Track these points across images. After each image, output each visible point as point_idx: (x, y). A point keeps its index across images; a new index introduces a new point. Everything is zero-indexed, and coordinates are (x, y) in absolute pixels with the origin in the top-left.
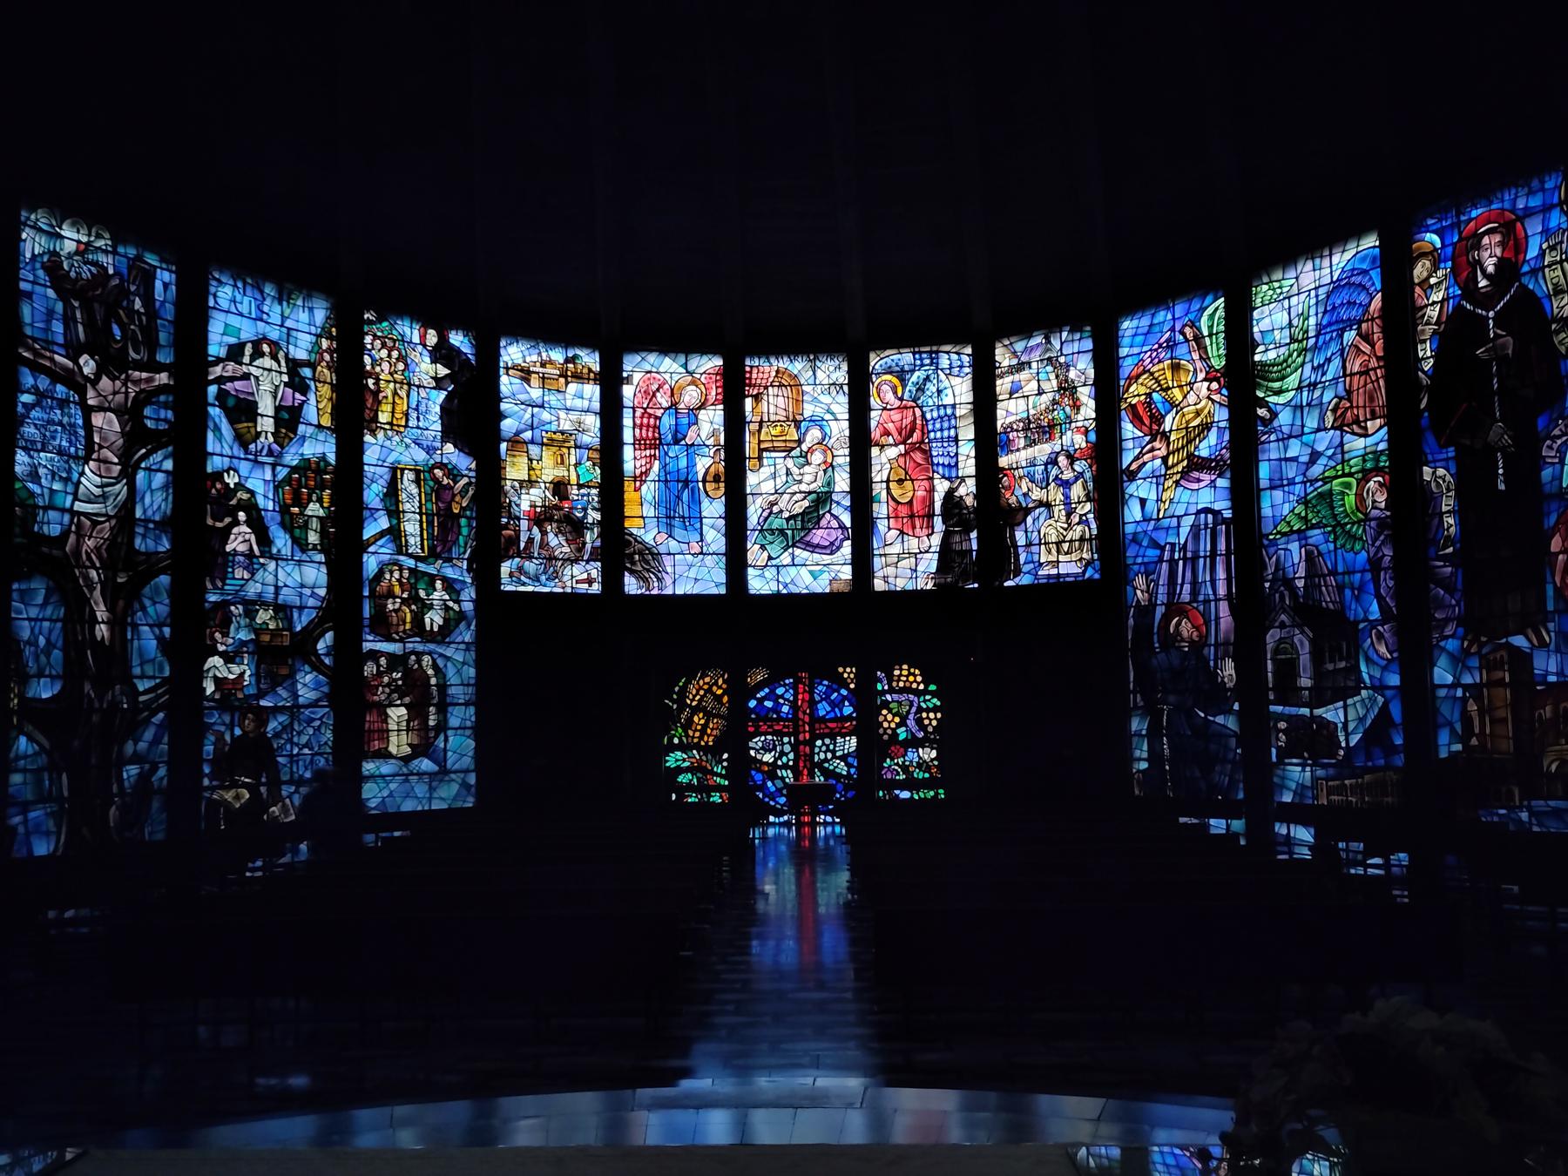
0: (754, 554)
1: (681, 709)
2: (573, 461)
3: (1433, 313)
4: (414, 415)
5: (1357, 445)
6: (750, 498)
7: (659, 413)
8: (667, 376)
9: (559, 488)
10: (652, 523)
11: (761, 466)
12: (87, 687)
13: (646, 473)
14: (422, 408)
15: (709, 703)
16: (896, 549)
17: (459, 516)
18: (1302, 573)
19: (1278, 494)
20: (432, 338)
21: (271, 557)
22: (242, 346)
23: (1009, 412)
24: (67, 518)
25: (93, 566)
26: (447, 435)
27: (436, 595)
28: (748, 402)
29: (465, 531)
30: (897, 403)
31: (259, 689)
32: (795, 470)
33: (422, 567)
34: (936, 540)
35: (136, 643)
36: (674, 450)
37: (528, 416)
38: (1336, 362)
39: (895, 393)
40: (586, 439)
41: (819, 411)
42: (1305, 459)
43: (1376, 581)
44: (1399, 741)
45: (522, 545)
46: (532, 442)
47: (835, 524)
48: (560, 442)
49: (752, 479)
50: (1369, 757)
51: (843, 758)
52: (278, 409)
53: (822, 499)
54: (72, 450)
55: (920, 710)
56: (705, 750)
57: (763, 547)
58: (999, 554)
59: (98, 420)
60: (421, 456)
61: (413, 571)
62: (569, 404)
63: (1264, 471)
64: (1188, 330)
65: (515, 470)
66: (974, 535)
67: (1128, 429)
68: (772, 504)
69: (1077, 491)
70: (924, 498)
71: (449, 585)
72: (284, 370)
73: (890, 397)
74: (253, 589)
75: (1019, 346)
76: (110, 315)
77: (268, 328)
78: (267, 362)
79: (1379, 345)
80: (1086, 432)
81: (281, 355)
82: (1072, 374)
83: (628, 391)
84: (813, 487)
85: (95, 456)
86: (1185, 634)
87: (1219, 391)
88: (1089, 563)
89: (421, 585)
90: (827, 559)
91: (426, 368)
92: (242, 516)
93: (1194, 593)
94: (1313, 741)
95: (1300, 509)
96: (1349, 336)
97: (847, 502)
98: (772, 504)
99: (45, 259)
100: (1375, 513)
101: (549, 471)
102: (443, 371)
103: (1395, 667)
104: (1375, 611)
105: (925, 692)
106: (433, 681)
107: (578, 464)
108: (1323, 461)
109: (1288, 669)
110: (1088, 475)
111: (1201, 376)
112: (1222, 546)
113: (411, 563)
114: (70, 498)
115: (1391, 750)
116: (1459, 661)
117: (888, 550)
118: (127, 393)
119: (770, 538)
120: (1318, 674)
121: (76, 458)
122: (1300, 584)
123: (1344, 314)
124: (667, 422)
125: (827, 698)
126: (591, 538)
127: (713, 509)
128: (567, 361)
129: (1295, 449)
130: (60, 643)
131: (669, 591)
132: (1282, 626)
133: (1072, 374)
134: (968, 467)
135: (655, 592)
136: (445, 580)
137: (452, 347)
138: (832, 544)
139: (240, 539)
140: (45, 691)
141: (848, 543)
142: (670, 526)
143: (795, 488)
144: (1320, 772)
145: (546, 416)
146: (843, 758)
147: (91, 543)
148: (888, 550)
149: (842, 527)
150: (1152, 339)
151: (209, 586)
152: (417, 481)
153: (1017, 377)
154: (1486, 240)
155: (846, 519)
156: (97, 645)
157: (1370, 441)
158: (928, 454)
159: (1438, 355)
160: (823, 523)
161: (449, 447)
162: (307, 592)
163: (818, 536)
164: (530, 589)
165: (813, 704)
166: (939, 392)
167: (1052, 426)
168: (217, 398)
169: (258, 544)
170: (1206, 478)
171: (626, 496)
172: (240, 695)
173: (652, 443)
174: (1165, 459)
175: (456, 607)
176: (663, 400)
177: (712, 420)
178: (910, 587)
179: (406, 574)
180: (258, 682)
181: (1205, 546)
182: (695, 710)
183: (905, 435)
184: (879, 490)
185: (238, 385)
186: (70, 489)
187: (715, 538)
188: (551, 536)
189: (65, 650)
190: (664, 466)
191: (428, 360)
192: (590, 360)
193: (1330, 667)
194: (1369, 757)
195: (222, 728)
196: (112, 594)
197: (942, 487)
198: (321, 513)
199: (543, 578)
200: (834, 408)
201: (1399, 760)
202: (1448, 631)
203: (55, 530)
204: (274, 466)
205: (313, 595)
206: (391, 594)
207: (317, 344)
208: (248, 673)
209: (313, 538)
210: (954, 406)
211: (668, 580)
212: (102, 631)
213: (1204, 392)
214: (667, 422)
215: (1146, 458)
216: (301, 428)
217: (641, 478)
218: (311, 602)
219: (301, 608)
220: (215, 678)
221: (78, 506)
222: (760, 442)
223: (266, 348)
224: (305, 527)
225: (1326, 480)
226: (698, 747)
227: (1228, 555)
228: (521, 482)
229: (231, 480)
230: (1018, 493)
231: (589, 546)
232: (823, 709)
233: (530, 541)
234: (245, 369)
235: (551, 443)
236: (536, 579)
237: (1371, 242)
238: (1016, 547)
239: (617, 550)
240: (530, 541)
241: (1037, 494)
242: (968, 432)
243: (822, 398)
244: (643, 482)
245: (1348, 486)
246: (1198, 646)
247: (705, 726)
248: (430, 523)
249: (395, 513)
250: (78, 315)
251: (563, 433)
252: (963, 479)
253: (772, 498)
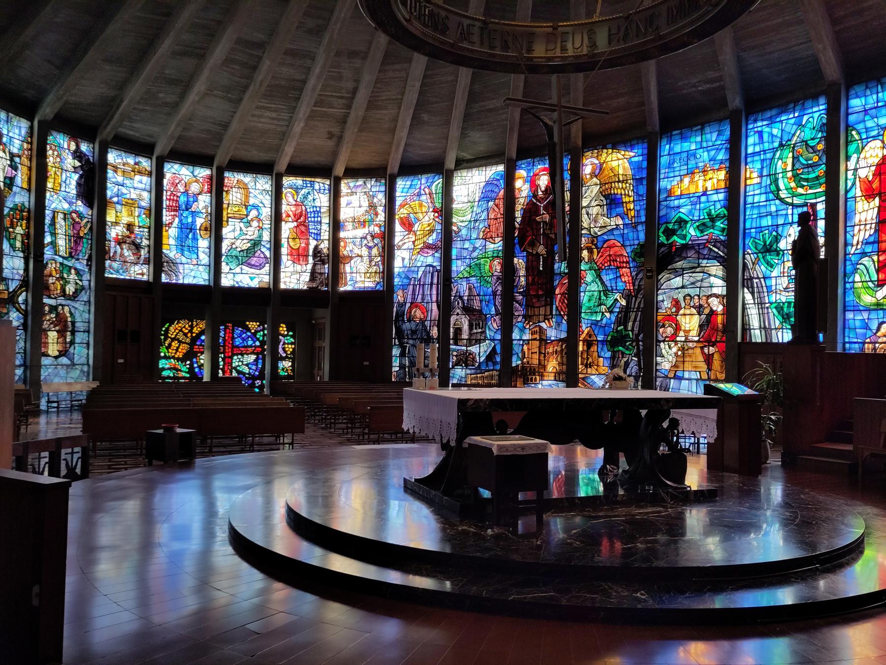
0: (225, 268)
1: (165, 339)
2: (137, 214)
3: (522, 201)
4: (64, 185)
5: (491, 246)
7: (179, 194)
8: (183, 177)
9: (130, 227)
10: (174, 248)
13: (171, 223)
14: (68, 182)
15: (181, 336)
17: (82, 238)
18: (467, 294)
19: (459, 262)
20: (73, 146)
23: (345, 213)
26: (79, 195)
27: (72, 277)
29: (85, 245)
30: (294, 203)
32: (244, 229)
33: (66, 262)
34: (309, 267)
36: (185, 214)
37: (116, 190)
38: (485, 213)
40: (143, 204)
41: (257, 202)
42: (471, 249)
43: (494, 299)
44: (498, 359)
45: (112, 254)
46: (118, 203)
47: (262, 256)
48: (131, 204)
49: (225, 231)
50: (487, 365)
51: (247, 365)
53: (256, 243)
55: (284, 343)
56: (178, 359)
57: (227, 264)
58: (336, 276)
60: (66, 206)
61: (61, 264)
62: (136, 185)
63: (454, 252)
64: (427, 190)
65: (110, 217)
66: (326, 266)
67: (398, 227)
68: (233, 244)
69: (375, 251)
71: (78, 272)
73: (291, 199)
75: (352, 185)
79: (502, 209)
80: (380, 227)
81: (7, 150)
82: (375, 200)
83: (165, 182)
84: (252, 237)
86: (418, 316)
87: (437, 217)
88: (378, 283)
89: (65, 271)
90: (258, 272)
91: (70, 162)
93: (423, 299)
94: (466, 360)
95: (468, 269)
96: (491, 204)
98: (233, 244)
100: (496, 274)
101: (125, 219)
102: (78, 164)
103: (499, 332)
104: (493, 311)
105: (287, 335)
106: (69, 319)
107: (139, 216)
108: (478, 251)
109: (458, 331)
110: (380, 245)
111: (431, 210)
112: (638, 319)
113: (61, 260)
115: (495, 363)
116: (522, 330)
117: (286, 270)
120: (471, 334)
122: (466, 298)
123: (489, 194)
124: (183, 199)
125: (240, 336)
126: (144, 253)
127: (204, 244)
128: (136, 164)
129: (467, 245)
131: (181, 282)
132: (458, 314)
133: (375, 200)
134: (325, 235)
135: (174, 281)
136: (76, 269)
137: (81, 152)
141: (267, 265)
142: (182, 250)
143: (244, 237)
144: (469, 372)
145: (124, 190)
146: (247, 365)
149: (266, 257)
150: (411, 191)
152: (65, 219)
153: (350, 198)
154: (542, 177)
155: (268, 254)
157: (496, 245)
158: (307, 227)
159: (523, 217)
160: (257, 255)
161: (79, 203)
162: (15, 271)
163: (253, 261)
164: (114, 276)
165: (233, 338)
166: (314, 200)
167: (364, 222)
170: (431, 252)
174: (414, 242)
175: (80, 283)
176: (181, 188)
177: (204, 201)
178: (296, 287)
179: (58, 265)
181: (428, 280)
182: (173, 340)
183: (297, 217)
184: (284, 242)
187: (204, 259)
188: (125, 251)
190: (181, 221)
191: (70, 157)
192: (145, 163)
193: (475, 331)
194: (487, 365)
197: (313, 243)
198: (22, 232)
199: (121, 271)
200: (264, 201)
201: (498, 367)
202: (519, 320)
205: (18, 273)
206: (51, 275)
207: (22, 146)
209: (18, 244)
210: (320, 207)
211: (181, 277)
213: (432, 217)
214: (183, 199)
215: (406, 241)
216: (14, 188)
218: (17, 277)
219: (12, 280)
224: (15, 239)
225: (478, 259)
226: (173, 357)
227: (438, 284)
228: (112, 222)
230: (348, 249)
231: (142, 257)
232: (238, 342)
233: (115, 252)
235: (127, 204)
236: (118, 271)
237: (501, 168)
238: (346, 273)
239: (158, 260)
240: (115, 252)
241: (357, 251)
242: (326, 220)
244: (170, 227)
245: (487, 262)
246: (423, 321)
247: (178, 348)
248: (70, 240)
249: (54, 234)
251: (132, 199)
252: (323, 241)
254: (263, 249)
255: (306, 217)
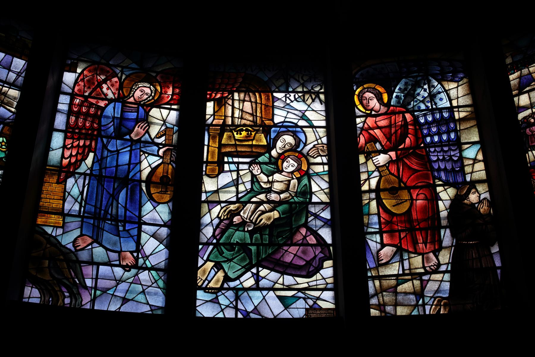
0: (206, 270)
6: (205, 208)
7: (102, 104)
10: (74, 223)
11: (222, 171)
13: (78, 164)
16: (394, 269)
28: (210, 107)
30: (383, 109)
32: (263, 178)
34: (445, 257)
39: (380, 99)
41: (292, 118)
47: (312, 240)
53: (297, 208)
57: (218, 266)
68: (233, 214)
70: (424, 209)
73: (374, 103)
90: (303, 282)
97: (326, 215)
98: (236, 213)
117: (384, 271)
119: (227, 253)
127: (157, 212)
138: (309, 263)
141: (328, 263)
143: (262, 197)
148: (384, 271)
155: (326, 234)
160: (298, 238)
163: (290, 254)
171: (46, 187)
173: (87, 130)
183: (393, 140)
187: (155, 250)
197: (446, 195)
200: (310, 115)
217: (66, 171)
222: (221, 146)
243: (295, 104)
252: (473, 184)
253: (232, 207)
254: (314, 223)
255: (419, 137)
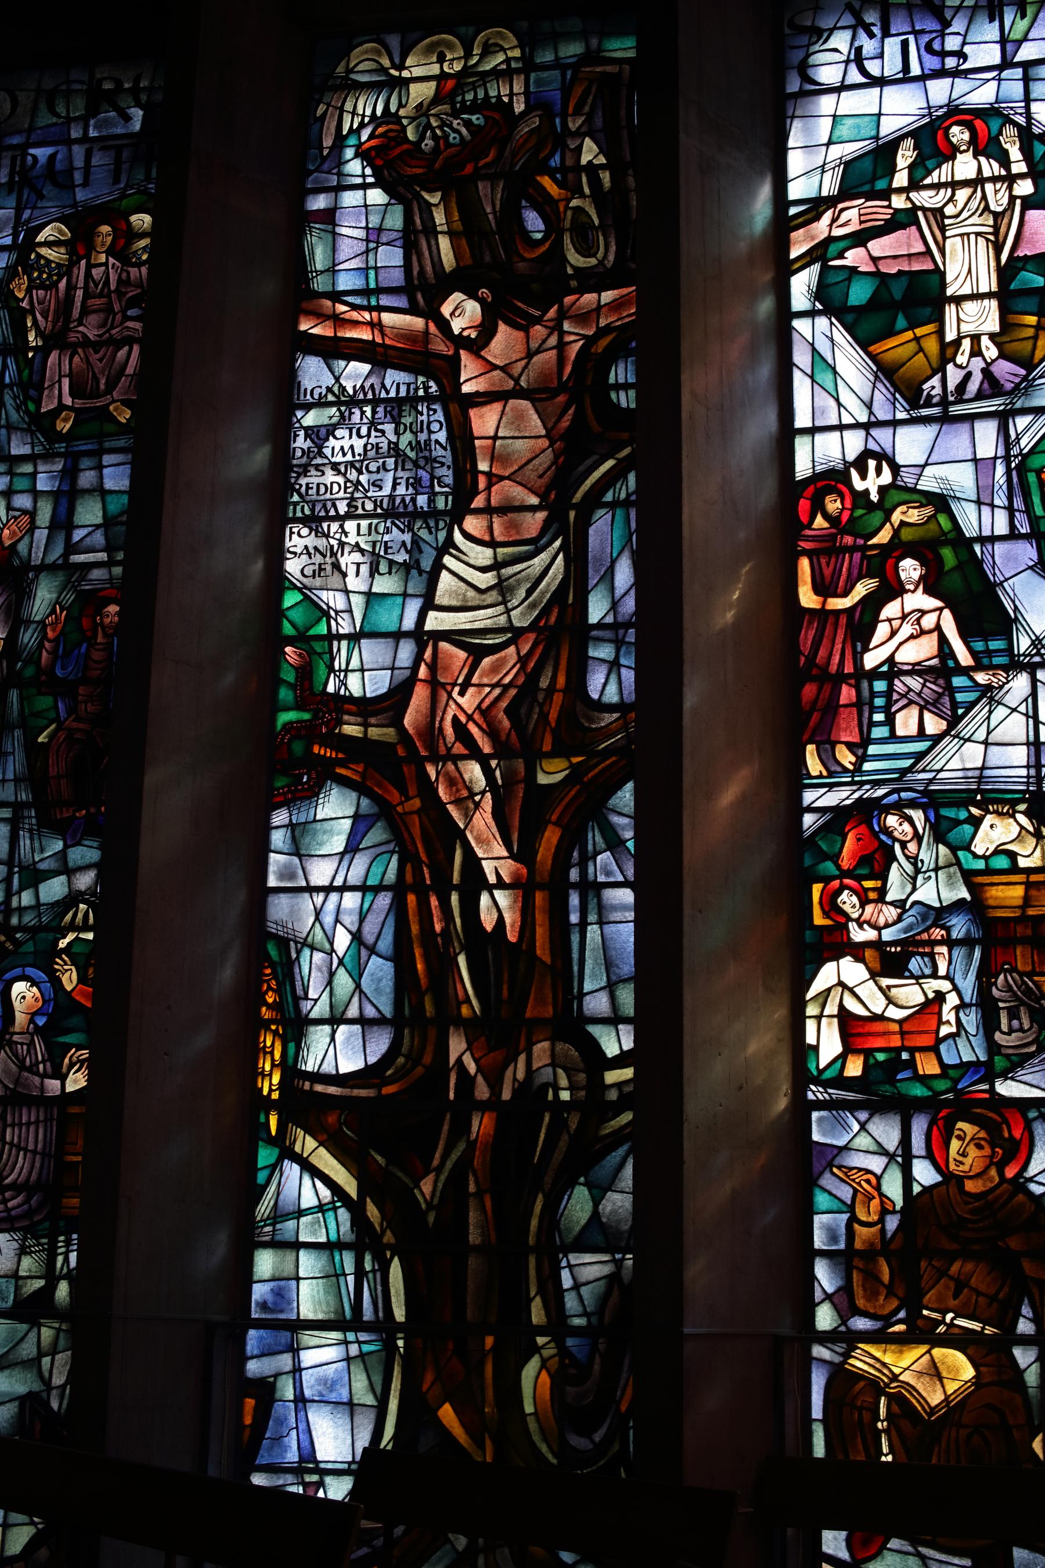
12: (456, 1046)
21: (1015, 665)
22: (883, 153)
24: (406, 652)
25: (475, 753)
31: (993, 1048)
35: (593, 932)
52: (1006, 273)
54: (422, 500)
59: (485, 421)
72: (1019, 167)
74: (957, 761)
76: (522, 190)
77: (962, 85)
78: (965, 166)
85: (478, 502)
92: (910, 569)
99: (365, 135)
114: (413, 608)
118: (561, 347)
121: (433, 513)
130: (386, 944)
139: (907, 630)
140: (338, 1052)
147: (468, 701)
151: (814, 765)
156: (483, 944)
168: (821, 292)
169: (965, 635)
172: (928, 1066)
180: (989, 1025)
185: (878, 247)
186: (416, 585)
189: (401, 957)
195: (876, 1164)
196: (523, 816)
203: (376, 684)
204: (1004, 418)
208: (952, 1000)
212: (497, 907)
220: (844, 1016)
221: (435, 621)
223: (959, 134)
229: (871, 483)
234: (899, 202)
250: (439, 218)
